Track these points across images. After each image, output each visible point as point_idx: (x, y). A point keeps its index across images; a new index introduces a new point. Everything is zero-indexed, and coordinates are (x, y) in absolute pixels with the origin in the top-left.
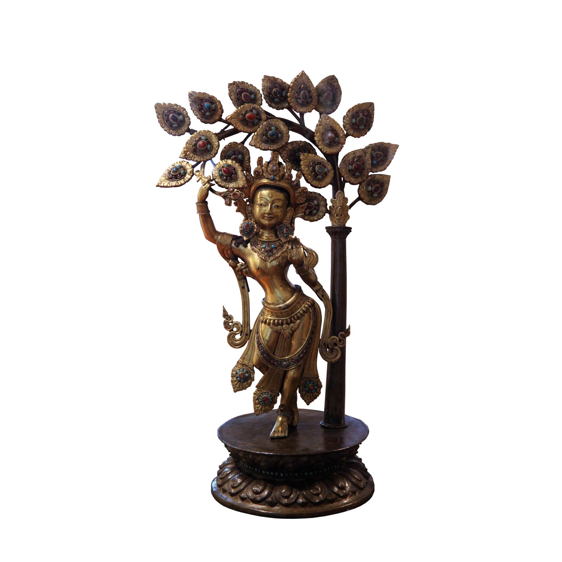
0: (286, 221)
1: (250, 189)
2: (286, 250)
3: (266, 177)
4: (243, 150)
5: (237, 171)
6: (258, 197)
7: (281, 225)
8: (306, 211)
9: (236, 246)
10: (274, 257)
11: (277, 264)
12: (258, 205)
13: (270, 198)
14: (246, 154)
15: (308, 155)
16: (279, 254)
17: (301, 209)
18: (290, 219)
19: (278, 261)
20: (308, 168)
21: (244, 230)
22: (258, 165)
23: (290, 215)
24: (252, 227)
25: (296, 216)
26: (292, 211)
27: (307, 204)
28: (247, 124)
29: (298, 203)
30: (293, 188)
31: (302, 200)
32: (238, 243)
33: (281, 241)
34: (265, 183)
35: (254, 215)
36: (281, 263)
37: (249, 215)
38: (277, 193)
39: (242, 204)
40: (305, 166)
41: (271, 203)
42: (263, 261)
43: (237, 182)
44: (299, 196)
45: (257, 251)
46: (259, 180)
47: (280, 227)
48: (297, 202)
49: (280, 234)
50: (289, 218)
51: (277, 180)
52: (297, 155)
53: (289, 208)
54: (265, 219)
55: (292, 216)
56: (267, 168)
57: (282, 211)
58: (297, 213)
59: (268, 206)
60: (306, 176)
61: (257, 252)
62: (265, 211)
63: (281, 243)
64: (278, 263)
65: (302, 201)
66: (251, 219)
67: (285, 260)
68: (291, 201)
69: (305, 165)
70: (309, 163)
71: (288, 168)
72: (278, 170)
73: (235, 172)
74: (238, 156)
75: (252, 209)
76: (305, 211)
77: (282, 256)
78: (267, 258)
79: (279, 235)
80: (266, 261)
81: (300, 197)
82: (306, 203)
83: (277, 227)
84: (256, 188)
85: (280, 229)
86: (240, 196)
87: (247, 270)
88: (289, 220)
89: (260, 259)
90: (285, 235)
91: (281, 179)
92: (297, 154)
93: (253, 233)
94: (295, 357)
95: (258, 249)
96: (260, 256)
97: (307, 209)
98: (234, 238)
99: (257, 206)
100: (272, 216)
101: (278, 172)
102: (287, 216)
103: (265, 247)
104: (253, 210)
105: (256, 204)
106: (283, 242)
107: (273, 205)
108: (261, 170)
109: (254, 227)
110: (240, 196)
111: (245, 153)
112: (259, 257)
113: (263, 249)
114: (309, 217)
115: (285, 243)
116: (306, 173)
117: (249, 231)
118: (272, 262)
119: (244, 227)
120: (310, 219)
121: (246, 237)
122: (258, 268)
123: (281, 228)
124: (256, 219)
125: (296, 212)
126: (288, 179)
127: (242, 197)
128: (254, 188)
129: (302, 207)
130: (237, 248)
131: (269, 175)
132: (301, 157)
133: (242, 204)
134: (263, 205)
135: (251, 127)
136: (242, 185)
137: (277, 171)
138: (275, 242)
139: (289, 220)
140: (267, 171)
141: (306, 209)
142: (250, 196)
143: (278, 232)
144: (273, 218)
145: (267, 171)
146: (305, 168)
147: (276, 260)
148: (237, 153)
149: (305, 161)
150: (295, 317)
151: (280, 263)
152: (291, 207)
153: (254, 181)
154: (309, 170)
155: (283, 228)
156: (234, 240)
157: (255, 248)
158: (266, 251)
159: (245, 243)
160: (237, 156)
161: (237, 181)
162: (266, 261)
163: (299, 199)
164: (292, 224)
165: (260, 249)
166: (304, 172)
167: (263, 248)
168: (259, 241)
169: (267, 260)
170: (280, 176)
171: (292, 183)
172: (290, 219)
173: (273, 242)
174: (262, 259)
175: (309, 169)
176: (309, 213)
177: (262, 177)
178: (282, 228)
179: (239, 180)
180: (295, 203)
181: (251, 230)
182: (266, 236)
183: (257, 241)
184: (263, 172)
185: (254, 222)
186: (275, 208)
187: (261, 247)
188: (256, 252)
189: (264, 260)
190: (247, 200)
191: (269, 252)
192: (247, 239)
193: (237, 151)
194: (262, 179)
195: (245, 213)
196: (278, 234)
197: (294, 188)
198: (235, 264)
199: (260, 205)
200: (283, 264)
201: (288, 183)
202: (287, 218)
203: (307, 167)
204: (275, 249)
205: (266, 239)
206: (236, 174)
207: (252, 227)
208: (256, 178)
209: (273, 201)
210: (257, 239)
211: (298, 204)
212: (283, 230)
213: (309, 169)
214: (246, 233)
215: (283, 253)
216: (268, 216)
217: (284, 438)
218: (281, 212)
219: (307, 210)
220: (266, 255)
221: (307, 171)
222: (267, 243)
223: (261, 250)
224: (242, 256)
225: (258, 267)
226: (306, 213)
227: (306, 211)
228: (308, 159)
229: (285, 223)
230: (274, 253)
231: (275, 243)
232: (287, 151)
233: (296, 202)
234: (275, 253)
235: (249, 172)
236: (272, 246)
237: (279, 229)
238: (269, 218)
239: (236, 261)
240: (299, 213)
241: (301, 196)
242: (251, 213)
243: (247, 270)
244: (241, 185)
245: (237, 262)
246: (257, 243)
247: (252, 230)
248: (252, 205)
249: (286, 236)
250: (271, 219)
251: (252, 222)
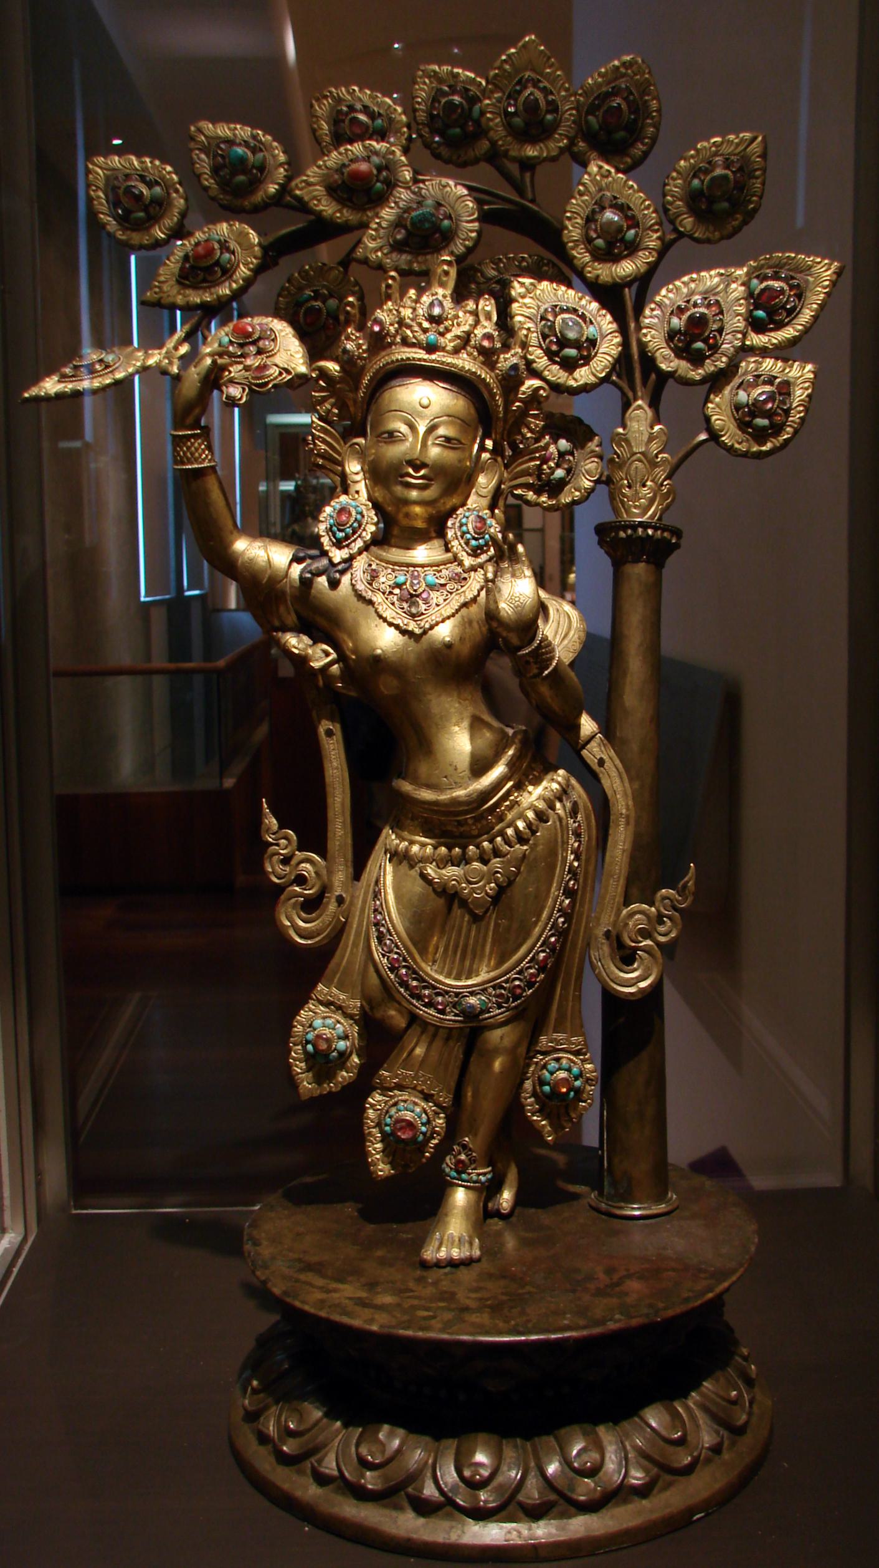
8: (545, 467)
28: (350, 200)
63: (459, 570)
76: (539, 467)
94: (506, 981)
115: (473, 569)
131: (421, 332)
135: (360, 208)
150: (510, 832)
217: (467, 1262)
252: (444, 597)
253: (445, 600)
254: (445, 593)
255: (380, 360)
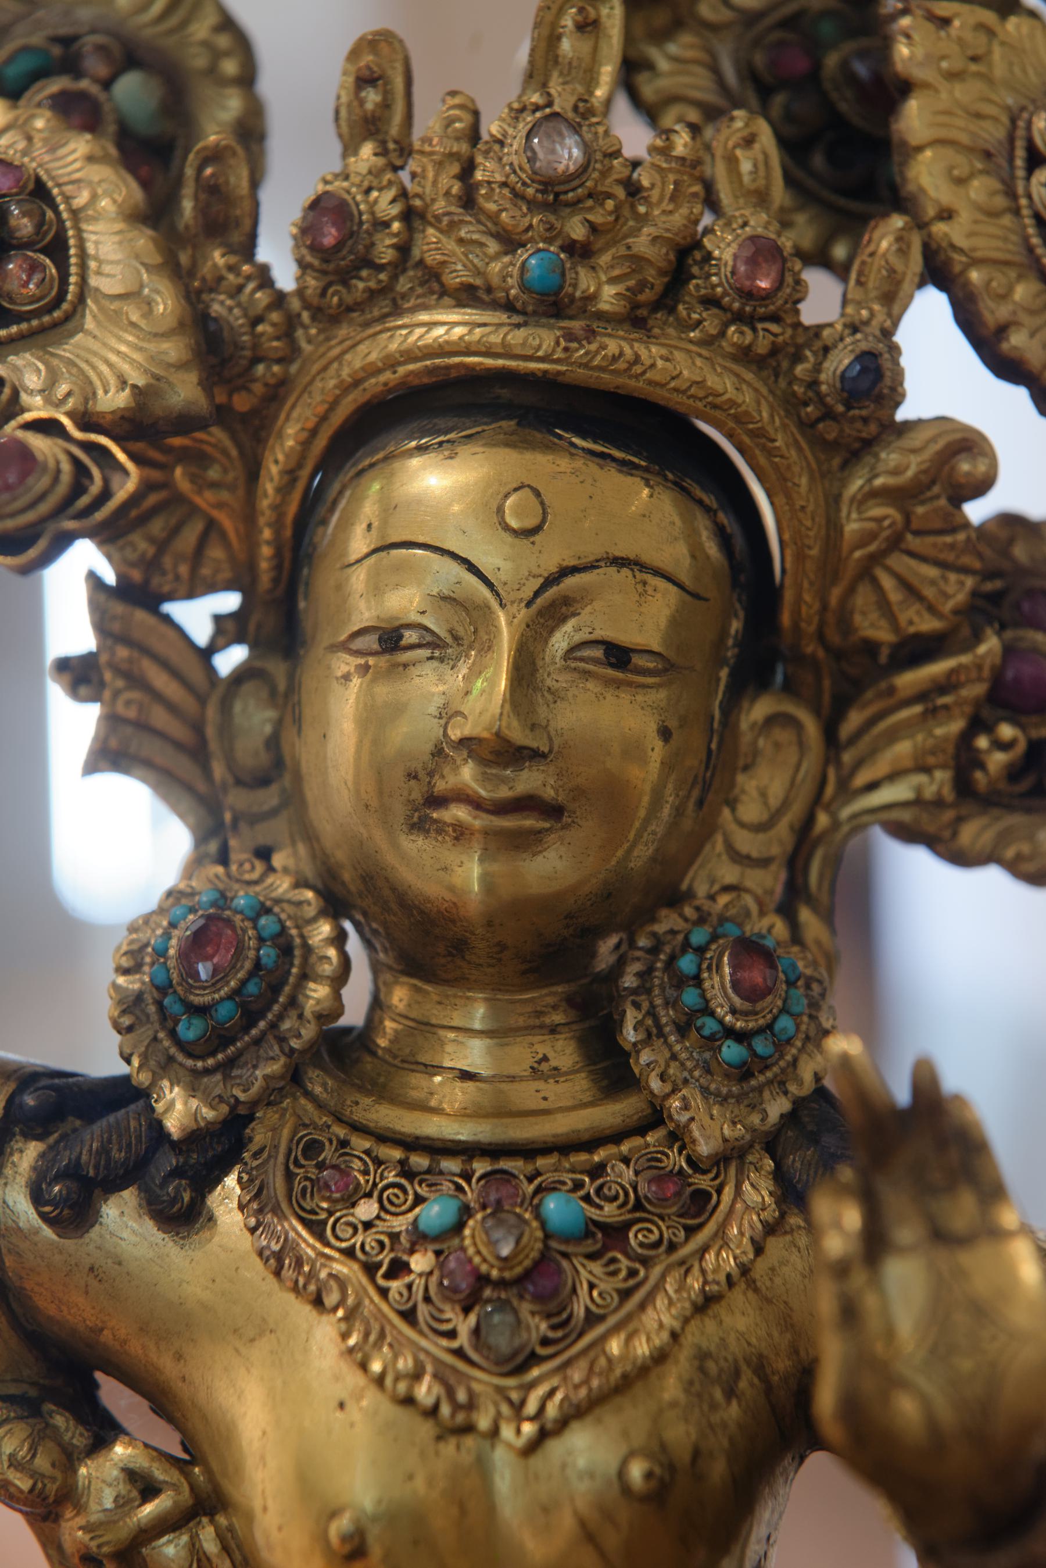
0: (729, 874)
1: (253, 473)
2: (745, 1270)
3: (458, 275)
4: (173, 21)
5: (75, 213)
6: (359, 544)
7: (668, 921)
9: (43, 1216)
10: (577, 1375)
11: (622, 1473)
12: (344, 647)
13: (508, 538)
14: (212, 71)
15: (991, 33)
16: (650, 1319)
17: (917, 709)
18: (775, 850)
19: (639, 1437)
20: (996, 185)
21: (163, 989)
22: (350, 148)
23: (774, 802)
24: (268, 954)
25: (845, 813)
26: (801, 745)
27: (990, 645)
29: (884, 635)
30: (807, 426)
31: (929, 592)
32: (73, 1173)
33: (678, 1137)
34: (442, 350)
35: (302, 803)
36: (684, 1456)
37: (237, 799)
38: (612, 479)
39: (160, 680)
40: (963, 164)
41: (523, 614)
42: (426, 1429)
43: (66, 351)
44: (895, 543)
45: (342, 1283)
46: (367, 325)
47: (654, 951)
48: (858, 618)
49: (653, 1034)
50: (760, 828)
51: (601, 316)
52: (845, 65)
53: (760, 709)
54: (440, 827)
55: (794, 813)
56: (468, 169)
57: (672, 724)
58: (861, 779)
59: (488, 647)
60: (974, 275)
61: (331, 1298)
62: (448, 714)
63: (675, 1160)
64: (636, 1471)
65: (932, 609)
66: (264, 854)
67: (734, 1410)
68: (786, 619)
69: (964, 139)
70: (1013, 121)
71: (746, 167)
72: (609, 185)
73: (40, 224)
74: (107, 84)
75: (279, 725)
77: (702, 1356)
78: (483, 1381)
79: (645, 1057)
80: (469, 1428)
81: (898, 561)
82: (977, 638)
83: (606, 948)
84: (321, 443)
85: (659, 976)
86: (78, 488)
87: (208, 1539)
88: (764, 863)
89: (389, 1410)
90: (731, 1051)
91: (656, 306)
92: (832, 61)
93: (282, 1040)
95: (349, 1253)
96: (376, 1367)
97: (986, 713)
98: (29, 1100)
99: (344, 663)
100: (549, 793)
101: (617, 210)
102: (732, 804)
103: (458, 1227)
104: (289, 735)
105: (325, 639)
106: (704, 1148)
107: (560, 641)
108: (385, 204)
109: (308, 949)
110: (78, 488)
111: (200, 61)
112: (354, 1379)
113: (420, 1262)
114: (1015, 819)
116: (986, 246)
117: (225, 1011)
118: (555, 1448)
119: (161, 953)
120: (1025, 848)
121: (192, 1090)
122: (345, 1539)
123: (672, 959)
124: (328, 842)
125: (847, 757)
126: (748, 294)
127: (106, 494)
128: (306, 444)
129: (922, 696)
130: (69, 1244)
132: (903, 50)
133: (160, 680)
134: (410, 637)
136: (139, 379)
137: (597, 196)
138: (590, 1144)
139: (764, 863)
140: (468, 200)
141: (977, 725)
142: (251, 566)
143: (631, 1016)
144: (553, 811)
145: (468, 200)
146: (961, 182)
147: (611, 1419)
148: (101, 49)
149: (962, 92)
151: (671, 1468)
152: (790, 688)
153: (293, 352)
154: (1017, 212)
155: (700, 950)
156: (29, 1135)
157: (308, 1244)
158: (465, 1285)
159: (177, 1173)
160: (94, 89)
161: (60, 342)
162: (469, 1428)
163: (887, 582)
164: (805, 915)
165: (386, 1258)
166: (940, 228)
167: (419, 1238)
168: (361, 1143)
169: (484, 1423)
170: (637, 261)
171: (797, 358)
172: (775, 850)
173: (564, 1147)
174: (409, 1401)
175: (1011, 194)
176: (1014, 773)
177: (403, 284)
178: (687, 963)
179: (89, 323)
180: (834, 638)
181: (252, 988)
182: (466, 1076)
183: (344, 1143)
184: (410, 216)
185: (300, 883)
186: (587, 674)
187: (400, 1224)
188: (318, 1302)
189: (433, 1412)
190: (219, 619)
191: (503, 1305)
192: (208, 1114)
193: (93, 31)
194: (397, 311)
195: (189, 788)
196: (630, 1035)
197: (829, 431)
198: (42, 1462)
199: (370, 642)
200: (718, 1470)
201: (745, 355)
202: (733, 827)
203: (979, 165)
204: (592, 1257)
205: (465, 1114)
206: (57, 249)
207: (268, 954)
208: (318, 312)
209: (550, 581)
210: (339, 1120)
211: (871, 647)
212: (697, 980)
213: (1011, 194)
214: (190, 1030)
215: (706, 1303)
216: (484, 779)
218: (665, 734)
219: (989, 728)
220: (463, 1339)
221: (993, 214)
222: (480, 1167)
223: (398, 1268)
224: (135, 1347)
225: (343, 1524)
226: (982, 766)
227: (982, 742)
228: (987, 79)
229: (723, 900)
230: (579, 1311)
231: (597, 1171)
232: (714, 28)
233: (845, 623)
234: (592, 1319)
235: (237, 237)
236: (553, 1205)
237: (645, 975)
238: (501, 808)
239: (59, 1420)
240: (893, 777)
241: (912, 541)
242: (263, 781)
243: (208, 1539)
244: (123, 383)
245: (77, 1436)
246: (344, 1172)
247: (275, 989)
248: (278, 669)
249: (744, 1072)
250: (529, 822)
251: (282, 885)
252: (619, 1282)
253: (625, 1294)
254: (624, 1263)
255: (339, 358)
